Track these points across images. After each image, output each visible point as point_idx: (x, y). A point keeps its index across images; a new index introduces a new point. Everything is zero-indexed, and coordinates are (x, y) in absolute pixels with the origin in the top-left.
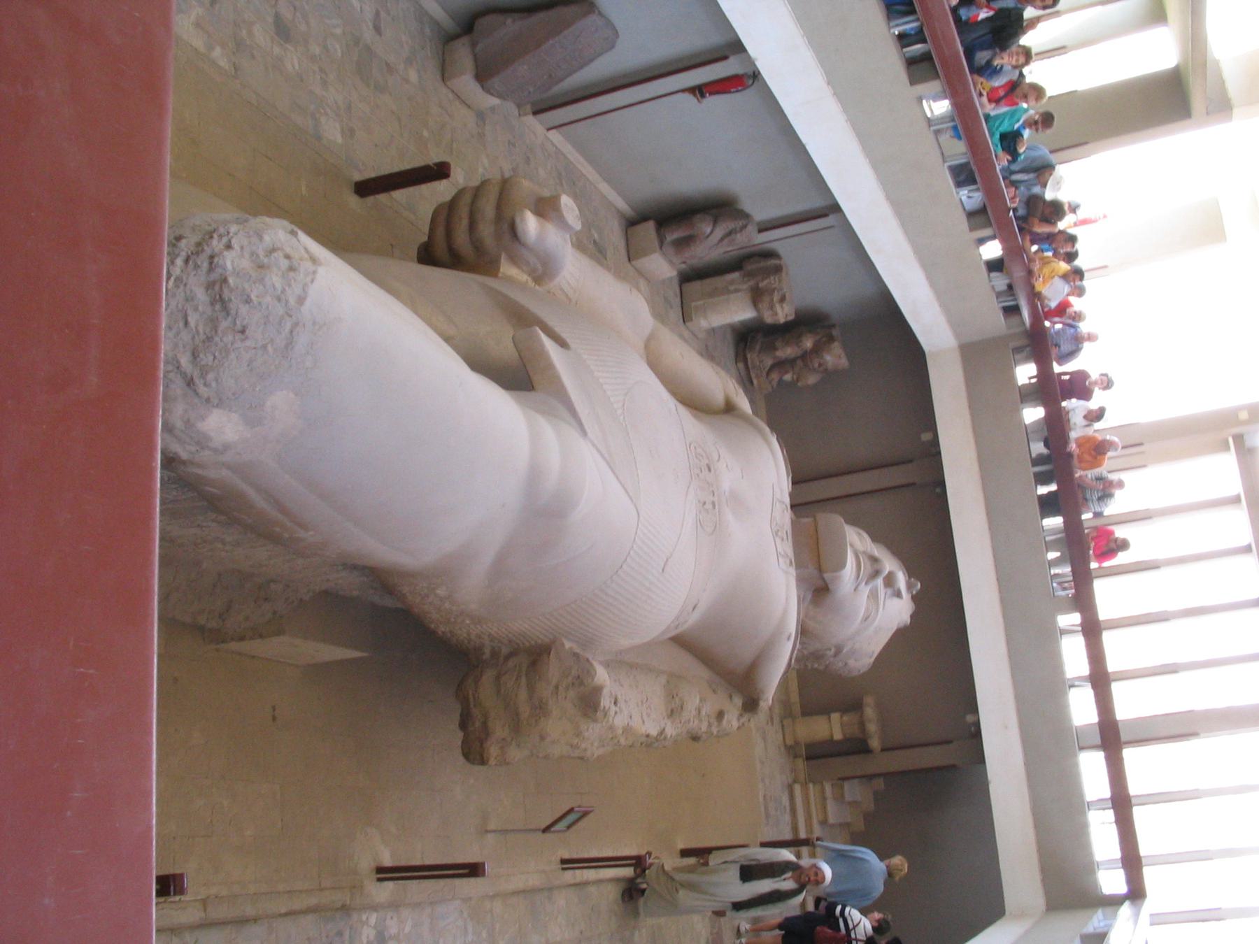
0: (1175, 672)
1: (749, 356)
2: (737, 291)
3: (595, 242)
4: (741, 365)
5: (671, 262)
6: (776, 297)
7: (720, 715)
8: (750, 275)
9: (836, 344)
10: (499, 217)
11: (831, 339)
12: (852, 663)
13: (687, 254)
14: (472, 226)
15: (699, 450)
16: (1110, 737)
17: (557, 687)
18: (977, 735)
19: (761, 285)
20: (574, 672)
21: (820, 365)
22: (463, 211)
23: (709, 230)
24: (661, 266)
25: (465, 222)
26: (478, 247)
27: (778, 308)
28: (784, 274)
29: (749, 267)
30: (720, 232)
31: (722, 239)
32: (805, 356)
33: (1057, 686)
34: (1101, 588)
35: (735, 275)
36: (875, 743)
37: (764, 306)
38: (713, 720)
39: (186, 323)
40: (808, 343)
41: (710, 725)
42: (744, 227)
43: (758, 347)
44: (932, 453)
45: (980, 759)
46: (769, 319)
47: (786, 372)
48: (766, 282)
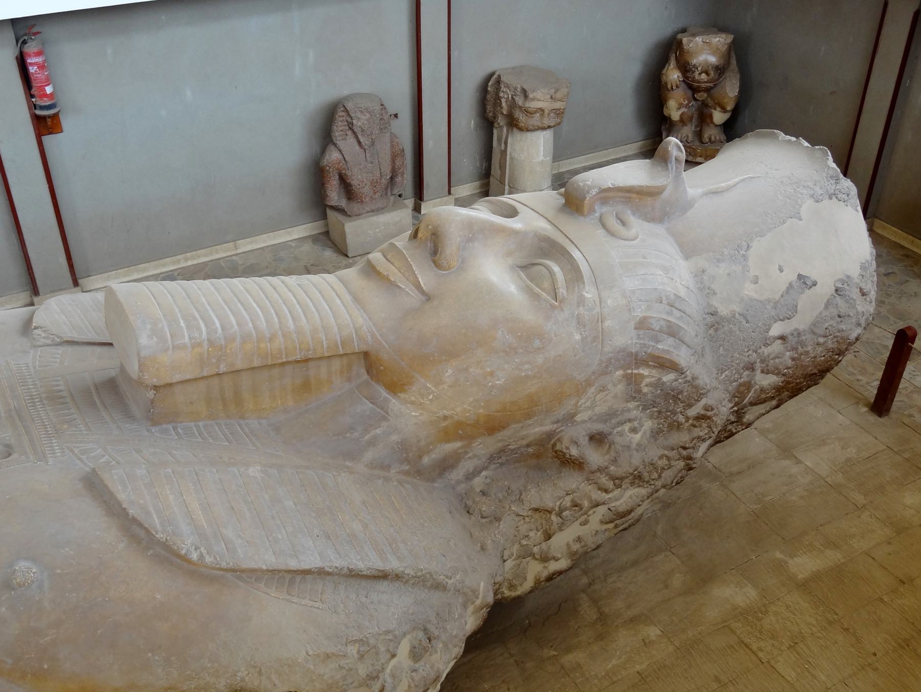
2: (506, 143)
6: (520, 101)
8: (495, 117)
9: (685, 40)
12: (776, 330)
13: (366, 190)
21: (707, 73)
27: (533, 105)
32: (692, 87)
35: (495, 132)
40: (673, 75)
47: (711, 116)
48: (503, 100)
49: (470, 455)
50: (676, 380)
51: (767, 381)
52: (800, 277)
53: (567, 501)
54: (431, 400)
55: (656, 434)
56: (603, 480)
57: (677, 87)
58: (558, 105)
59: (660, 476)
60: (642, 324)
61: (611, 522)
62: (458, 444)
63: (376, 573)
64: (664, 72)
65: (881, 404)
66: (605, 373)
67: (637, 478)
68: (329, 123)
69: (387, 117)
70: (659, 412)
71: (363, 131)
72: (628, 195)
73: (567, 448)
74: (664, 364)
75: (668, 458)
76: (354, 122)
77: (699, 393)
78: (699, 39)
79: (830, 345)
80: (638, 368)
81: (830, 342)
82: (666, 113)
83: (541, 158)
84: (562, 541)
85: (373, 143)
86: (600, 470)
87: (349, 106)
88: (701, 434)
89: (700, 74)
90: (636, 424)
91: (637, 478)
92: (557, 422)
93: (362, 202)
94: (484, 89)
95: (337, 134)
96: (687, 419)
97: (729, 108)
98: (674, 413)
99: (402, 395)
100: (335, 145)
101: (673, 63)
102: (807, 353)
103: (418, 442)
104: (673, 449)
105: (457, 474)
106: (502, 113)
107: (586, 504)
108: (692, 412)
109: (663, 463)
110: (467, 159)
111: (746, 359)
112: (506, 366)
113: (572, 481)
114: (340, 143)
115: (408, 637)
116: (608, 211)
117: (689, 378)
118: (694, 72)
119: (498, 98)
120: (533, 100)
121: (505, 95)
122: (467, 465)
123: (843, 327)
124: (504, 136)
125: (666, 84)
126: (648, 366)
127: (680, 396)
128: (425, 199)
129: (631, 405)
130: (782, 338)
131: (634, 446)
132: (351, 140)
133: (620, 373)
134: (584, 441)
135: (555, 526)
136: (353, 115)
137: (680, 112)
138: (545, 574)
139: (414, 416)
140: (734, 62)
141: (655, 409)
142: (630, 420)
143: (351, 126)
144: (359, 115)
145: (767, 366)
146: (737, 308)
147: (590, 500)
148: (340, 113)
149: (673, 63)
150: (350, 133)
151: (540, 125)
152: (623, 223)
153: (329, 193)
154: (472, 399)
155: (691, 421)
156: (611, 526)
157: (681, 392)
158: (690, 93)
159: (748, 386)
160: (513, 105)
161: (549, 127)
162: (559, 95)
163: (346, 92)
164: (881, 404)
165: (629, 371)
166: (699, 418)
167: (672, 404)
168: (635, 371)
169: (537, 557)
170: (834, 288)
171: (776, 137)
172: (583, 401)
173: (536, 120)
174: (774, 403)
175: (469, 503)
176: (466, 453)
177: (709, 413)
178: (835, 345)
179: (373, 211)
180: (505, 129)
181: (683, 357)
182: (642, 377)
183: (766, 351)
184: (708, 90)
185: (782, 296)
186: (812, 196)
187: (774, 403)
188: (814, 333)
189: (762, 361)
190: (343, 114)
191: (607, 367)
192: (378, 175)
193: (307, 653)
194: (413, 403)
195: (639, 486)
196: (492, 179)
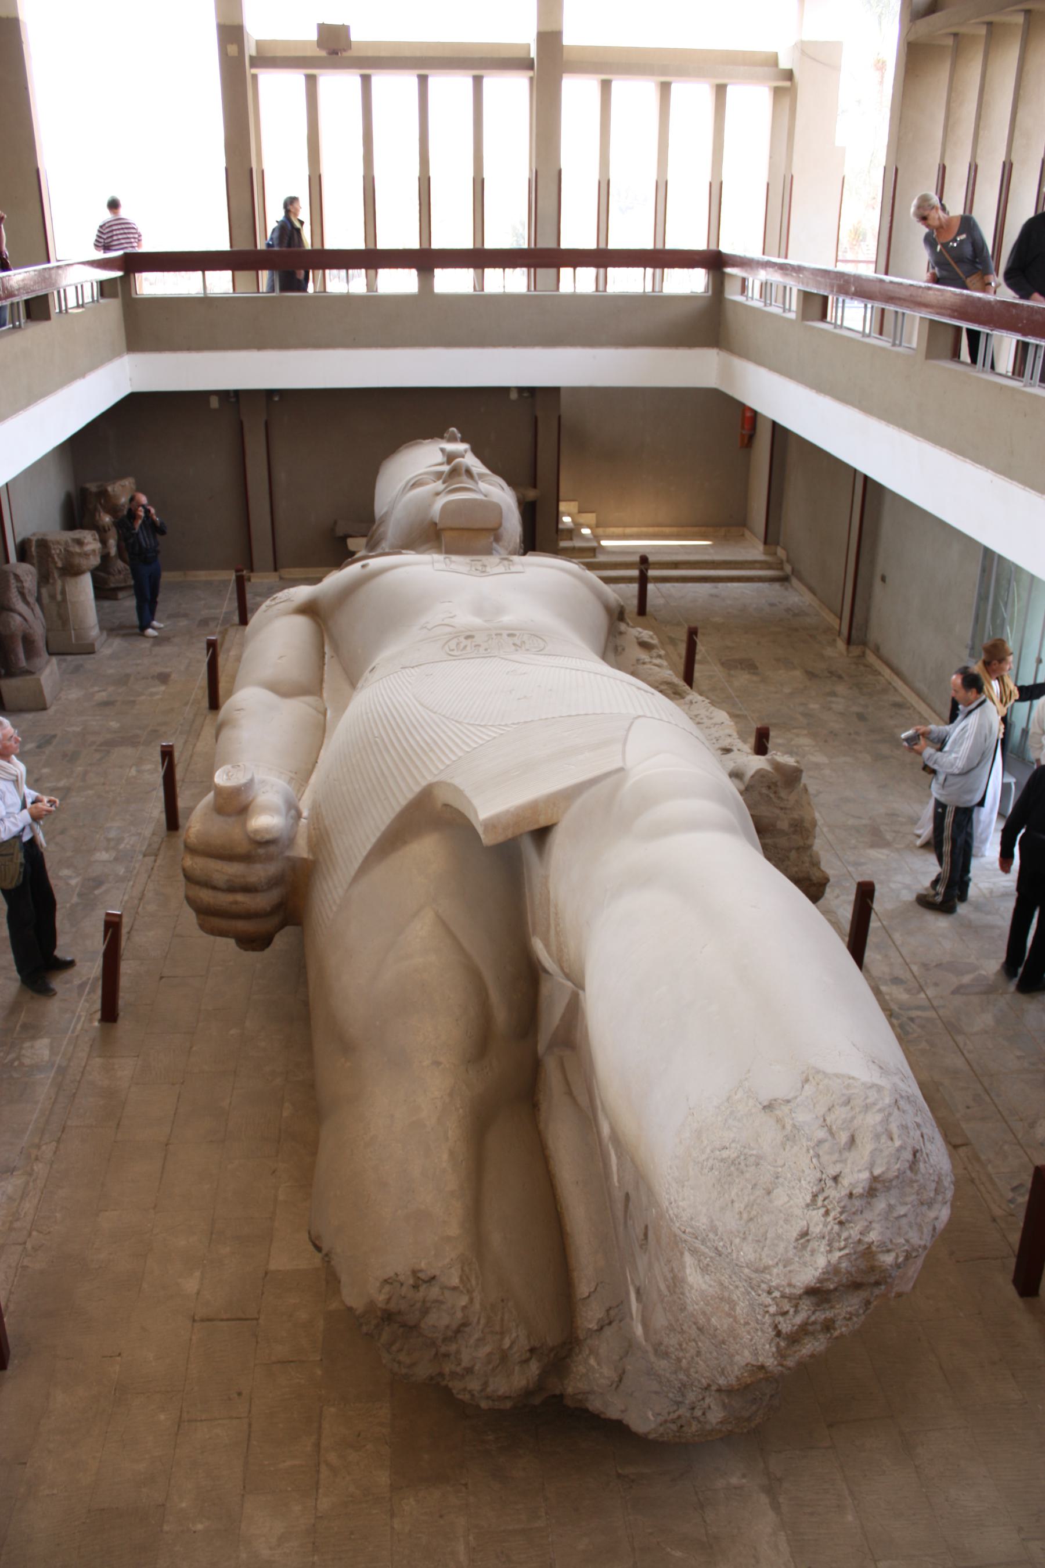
0: (789, 183)
1: (112, 585)
2: (63, 592)
3: (39, 747)
4: (121, 595)
5: (48, 662)
6: (77, 549)
7: (644, 645)
9: (110, 489)
10: (246, 858)
11: (103, 493)
14: (248, 889)
15: (453, 644)
16: (543, 257)
17: (781, 809)
18: (532, 391)
19: (60, 565)
20: (764, 791)
22: (224, 899)
23: (18, 618)
24: (49, 673)
25: (240, 897)
26: (275, 882)
27: (88, 548)
28: (49, 538)
30: (21, 606)
31: (27, 603)
33: (479, 303)
34: (333, 242)
36: (531, 494)
38: (654, 652)
39: (905, 1215)
42: (17, 577)
43: (102, 574)
44: (234, 400)
45: (555, 391)
46: (95, 561)
48: (56, 557)
120: (88, 543)
121: (55, 551)
148: (13, 581)
160: (69, 554)
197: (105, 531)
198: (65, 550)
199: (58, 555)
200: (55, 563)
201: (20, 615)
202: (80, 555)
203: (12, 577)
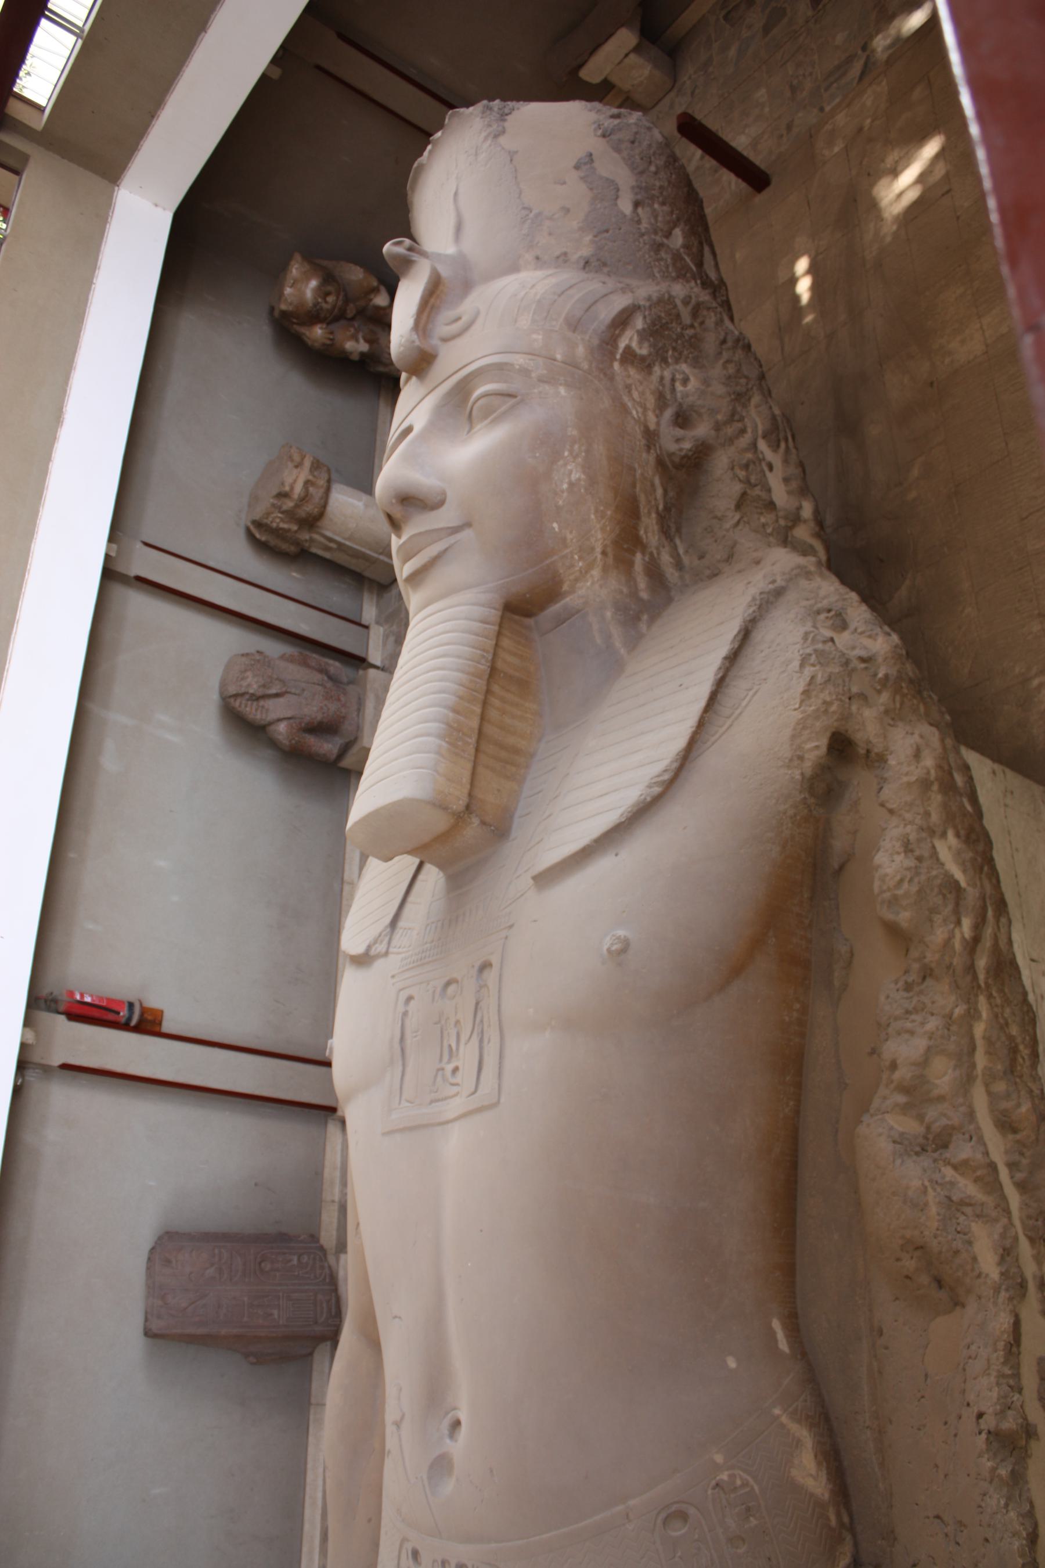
2: (331, 540)
6: (289, 504)
8: (297, 543)
9: (283, 307)
11: (284, 314)
12: (626, 206)
13: (333, 707)
21: (328, 294)
23: (282, 727)
27: (298, 489)
28: (258, 514)
29: (293, 549)
35: (314, 550)
37: (309, 508)
41: (927, 973)
42: (236, 696)
47: (378, 308)
48: (283, 525)
49: (655, 552)
50: (645, 317)
51: (678, 239)
52: (577, 167)
53: (742, 474)
54: (581, 558)
55: (696, 362)
56: (729, 431)
57: (332, 333)
58: (307, 463)
59: (746, 377)
60: (574, 325)
61: (779, 441)
62: (638, 558)
63: (740, 637)
64: (310, 343)
65: (757, 179)
66: (612, 379)
67: (740, 398)
68: (243, 724)
69: (257, 661)
70: (674, 349)
71: (264, 686)
72: (430, 305)
73: (681, 450)
74: (622, 321)
75: (728, 361)
76: (251, 691)
77: (665, 302)
78: (288, 291)
79: (660, 162)
80: (616, 347)
81: (658, 162)
82: (355, 357)
83: (360, 505)
84: (780, 494)
85: (283, 682)
86: (718, 427)
87: (232, 690)
88: (713, 319)
89: (326, 302)
90: (678, 376)
91: (740, 398)
92: (648, 448)
93: (344, 717)
94: (261, 547)
95: (258, 717)
96: (692, 326)
97: (375, 284)
98: (681, 336)
99: (565, 587)
100: (270, 724)
101: (303, 330)
102: (661, 187)
103: (621, 592)
104: (720, 353)
105: (671, 574)
106: (296, 532)
107: (749, 456)
108: (687, 319)
109: (731, 369)
110: (334, 595)
111: (647, 247)
112: (569, 467)
113: (721, 461)
114: (272, 716)
115: (819, 625)
116: (442, 327)
117: (647, 304)
118: (321, 308)
119: (277, 532)
120: (292, 488)
121: (277, 521)
122: (666, 558)
123: (645, 143)
124: (322, 540)
125: (324, 344)
126: (619, 336)
127: (664, 321)
128: (363, 655)
129: (657, 369)
130: (637, 204)
131: (703, 387)
132: (269, 703)
133: (616, 365)
134: (679, 432)
135: (764, 495)
136: (243, 690)
137: (362, 341)
138: (812, 524)
139: (593, 583)
140: (325, 263)
141: (670, 353)
142: (673, 380)
143: (256, 698)
144: (244, 683)
145: (662, 230)
146: (588, 238)
147: (746, 450)
148: (236, 704)
149: (303, 330)
150: (262, 703)
151: (322, 491)
152: (459, 319)
153: (322, 751)
154: (593, 516)
155: (696, 324)
156: (783, 445)
157: (660, 317)
158: (343, 322)
159: (677, 257)
160: (290, 515)
161: (329, 481)
162: (297, 458)
163: (215, 696)
164: (757, 179)
165: (618, 356)
166: (695, 313)
167: (668, 335)
168: (620, 351)
169: (790, 524)
170: (601, 139)
171: (421, 167)
172: (634, 412)
173: (316, 493)
174: (706, 249)
175: (708, 572)
176: (651, 554)
177: (693, 301)
178: (664, 158)
179: (359, 710)
180: (316, 536)
181: (620, 302)
182: (628, 348)
183: (644, 225)
184: (347, 300)
185: (591, 189)
186: (496, 136)
187: (706, 249)
188: (642, 173)
189: (656, 233)
190: (238, 701)
191: (605, 374)
192: (320, 688)
193: (795, 710)
194: (577, 580)
195: (749, 400)
196: (367, 574)
197: (332, 345)
198: (282, 512)
199: (282, 520)
200: (289, 530)
201: (279, 720)
202: (297, 506)
203: (232, 700)
